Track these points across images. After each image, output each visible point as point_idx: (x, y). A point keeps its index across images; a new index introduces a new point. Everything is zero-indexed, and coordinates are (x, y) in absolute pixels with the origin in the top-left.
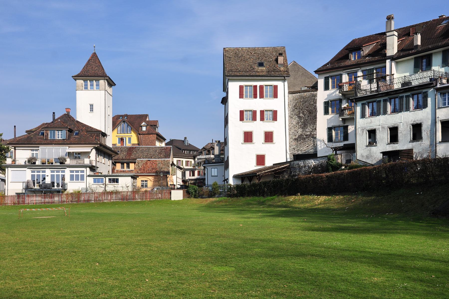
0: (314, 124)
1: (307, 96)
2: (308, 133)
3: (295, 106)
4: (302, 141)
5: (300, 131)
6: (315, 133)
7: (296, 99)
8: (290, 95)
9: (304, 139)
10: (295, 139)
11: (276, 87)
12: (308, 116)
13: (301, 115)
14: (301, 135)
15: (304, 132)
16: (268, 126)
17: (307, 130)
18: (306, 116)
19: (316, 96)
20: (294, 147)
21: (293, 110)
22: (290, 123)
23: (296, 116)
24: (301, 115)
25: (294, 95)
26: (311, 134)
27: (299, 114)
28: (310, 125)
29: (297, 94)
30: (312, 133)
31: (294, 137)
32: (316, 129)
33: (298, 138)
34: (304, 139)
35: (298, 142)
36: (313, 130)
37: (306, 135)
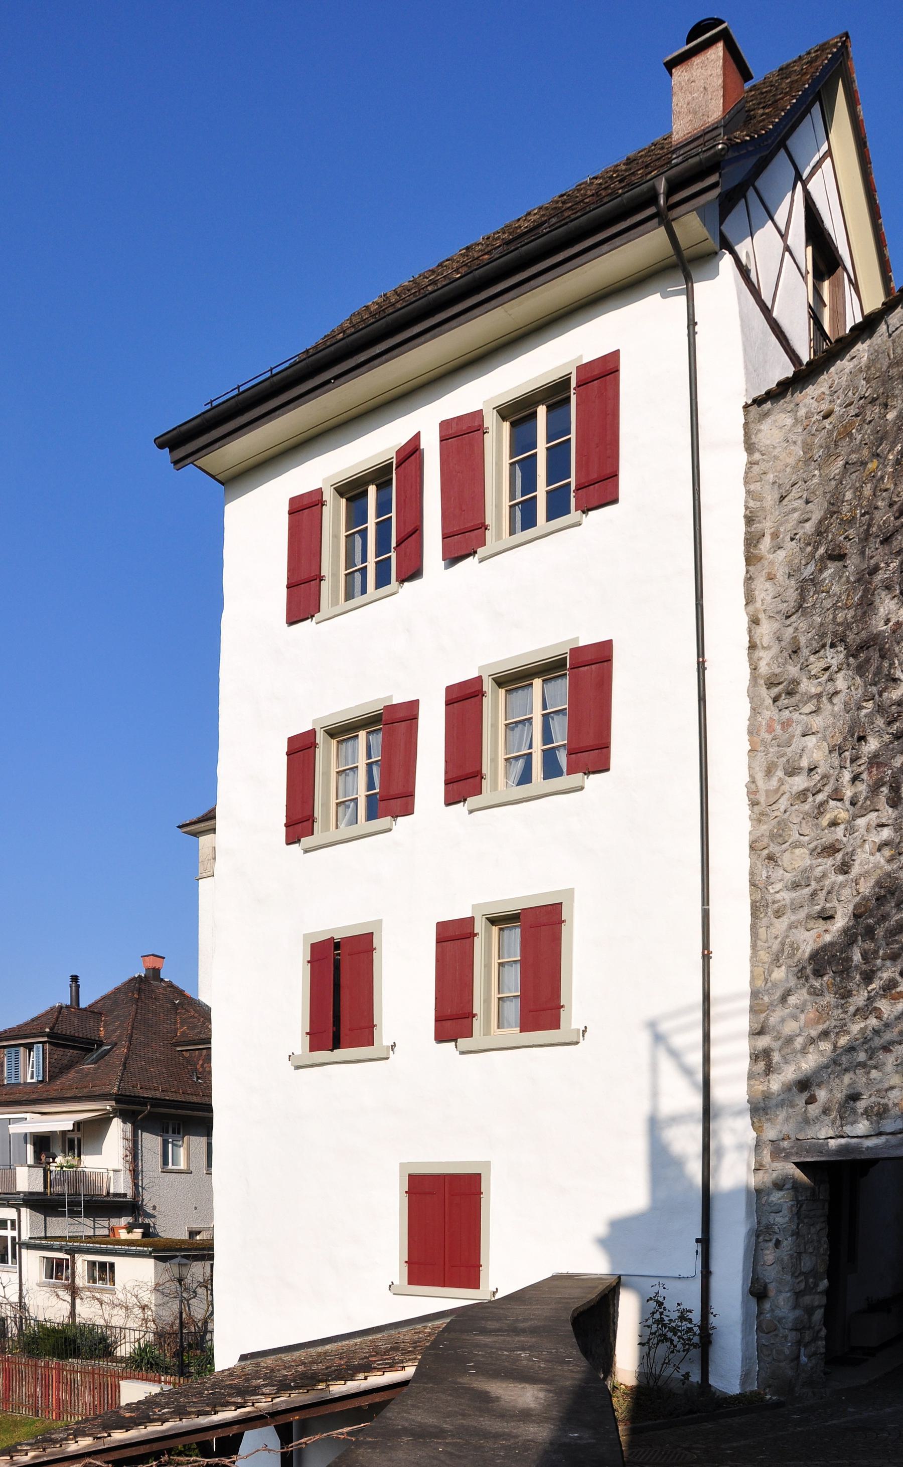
22: (771, 753)
23: (834, 657)
33: (849, 937)
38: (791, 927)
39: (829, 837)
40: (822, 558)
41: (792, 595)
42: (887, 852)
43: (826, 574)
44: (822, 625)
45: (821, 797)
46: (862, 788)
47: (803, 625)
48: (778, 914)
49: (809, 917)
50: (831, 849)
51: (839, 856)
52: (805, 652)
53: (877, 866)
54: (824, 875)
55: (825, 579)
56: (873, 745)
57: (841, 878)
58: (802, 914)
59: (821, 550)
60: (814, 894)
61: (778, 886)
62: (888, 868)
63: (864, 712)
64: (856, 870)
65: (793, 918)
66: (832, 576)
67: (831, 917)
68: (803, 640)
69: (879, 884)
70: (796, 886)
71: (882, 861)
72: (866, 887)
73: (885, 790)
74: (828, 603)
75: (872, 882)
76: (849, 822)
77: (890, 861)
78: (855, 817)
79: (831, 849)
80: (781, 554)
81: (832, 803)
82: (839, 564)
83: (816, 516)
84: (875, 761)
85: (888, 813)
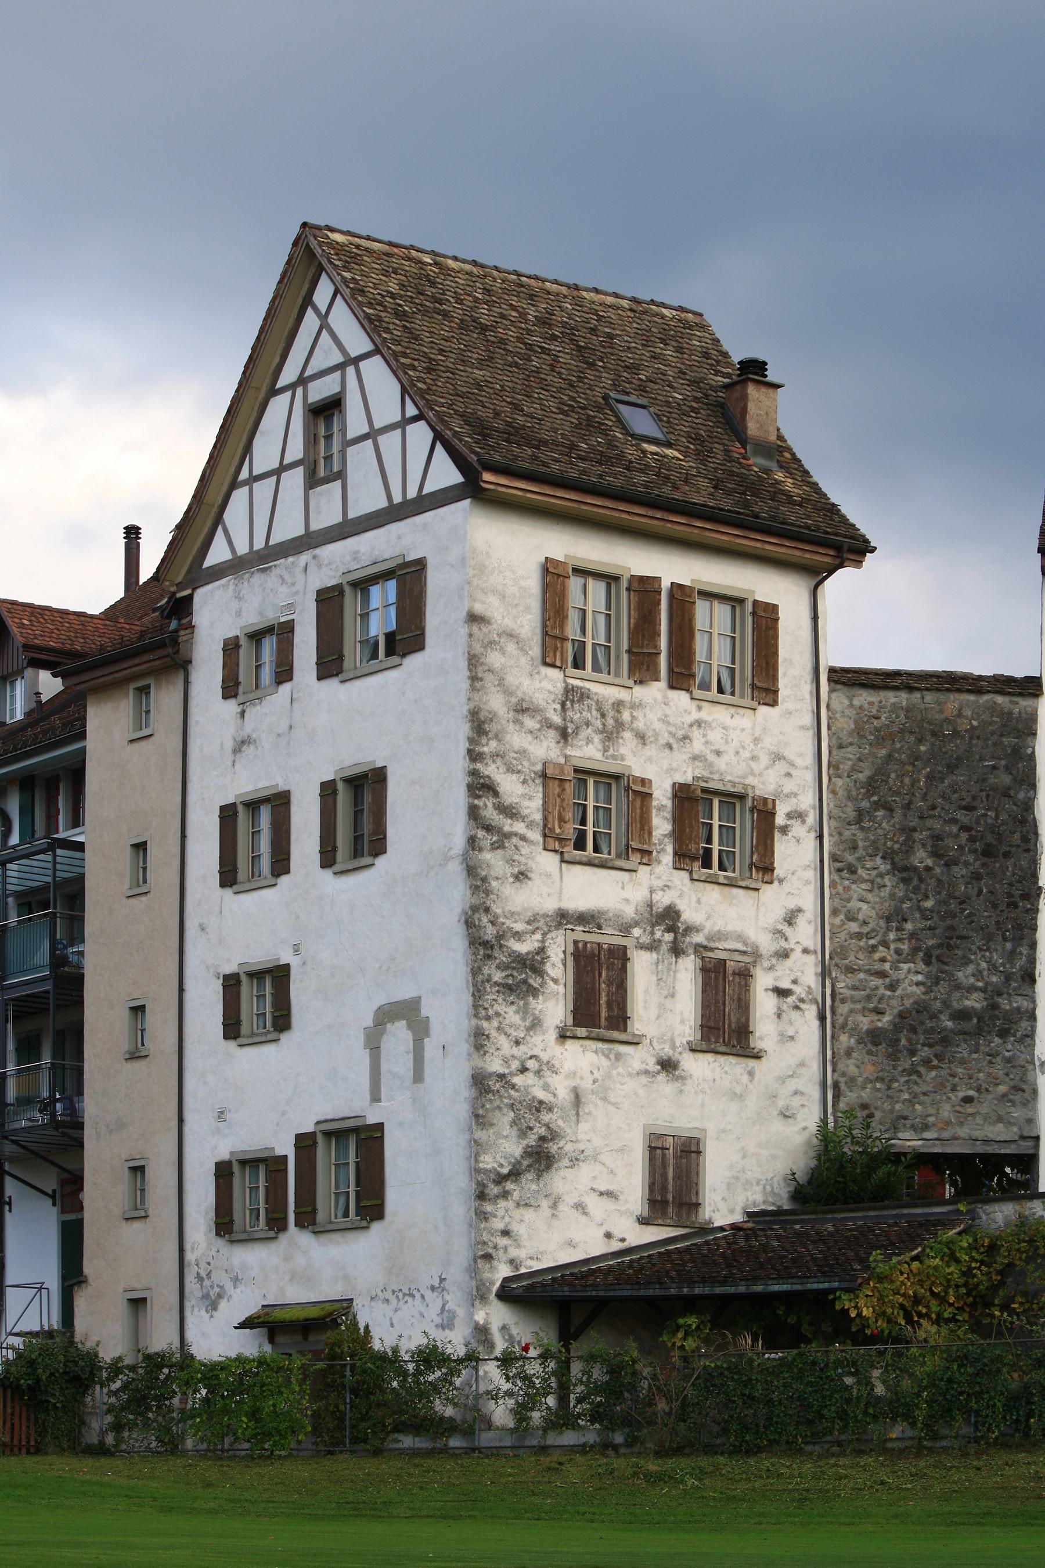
0: (1018, 940)
1: (963, 726)
2: (975, 1002)
3: (871, 786)
4: (925, 1052)
5: (911, 980)
6: (1025, 1004)
7: (882, 737)
8: (841, 700)
9: (945, 1041)
10: (874, 1036)
11: (765, 619)
12: (977, 877)
13: (921, 858)
14: (921, 1008)
15: (943, 988)
16: (721, 912)
17: (964, 975)
18: (959, 871)
19: (1028, 728)
20: (866, 1095)
21: (860, 814)
24: (921, 858)
25: (864, 698)
26: (994, 1006)
27: (908, 848)
28: (989, 938)
29: (891, 698)
30: (1004, 1004)
31: (865, 1022)
32: (1029, 977)
33: (897, 1027)
34: (945, 1041)
35: (893, 1057)
36: (1008, 977)
37: (962, 1015)
38: (851, 1011)
39: (877, 967)
40: (875, 802)
41: (851, 813)
42: (922, 988)
43: (877, 813)
44: (874, 842)
45: (872, 942)
46: (905, 947)
47: (860, 835)
48: (843, 1001)
49: (864, 1008)
50: (882, 974)
51: (888, 980)
52: (861, 852)
53: (913, 993)
54: (877, 988)
55: (877, 816)
56: (909, 926)
57: (888, 993)
58: (859, 1006)
59: (875, 798)
60: (869, 998)
61: (843, 985)
62: (923, 997)
63: (905, 906)
64: (899, 992)
65: (852, 1006)
66: (884, 817)
67: (883, 1013)
68: (861, 844)
69: (916, 1003)
70: (855, 988)
71: (918, 992)
72: (908, 1003)
73: (921, 954)
74: (880, 832)
75: (911, 1001)
76: (893, 962)
77: (924, 994)
78: (900, 962)
79: (882, 974)
80: (839, 782)
81: (881, 948)
82: (888, 813)
83: (867, 773)
84: (913, 935)
85: (921, 966)
